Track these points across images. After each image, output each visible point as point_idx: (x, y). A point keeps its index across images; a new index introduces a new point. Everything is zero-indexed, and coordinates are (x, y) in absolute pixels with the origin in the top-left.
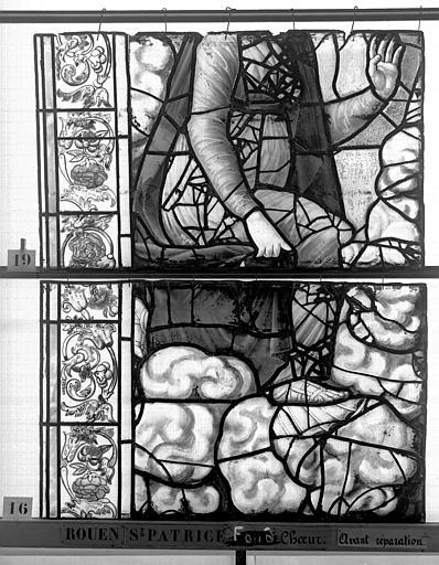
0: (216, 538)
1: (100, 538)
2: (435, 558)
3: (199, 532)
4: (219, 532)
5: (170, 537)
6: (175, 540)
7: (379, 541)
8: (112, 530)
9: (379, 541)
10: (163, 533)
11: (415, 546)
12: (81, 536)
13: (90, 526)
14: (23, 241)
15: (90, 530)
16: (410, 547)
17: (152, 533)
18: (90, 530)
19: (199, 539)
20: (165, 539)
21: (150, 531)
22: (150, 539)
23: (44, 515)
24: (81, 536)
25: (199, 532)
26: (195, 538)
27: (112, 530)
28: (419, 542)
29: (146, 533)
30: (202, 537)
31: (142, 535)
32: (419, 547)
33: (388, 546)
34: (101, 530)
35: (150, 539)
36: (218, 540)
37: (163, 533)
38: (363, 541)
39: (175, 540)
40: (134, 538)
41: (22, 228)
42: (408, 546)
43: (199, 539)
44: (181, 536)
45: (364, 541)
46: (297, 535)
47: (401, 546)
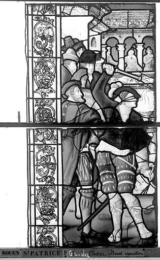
2: (159, 258)
9: (126, 254)
11: (140, 256)
14: (19, 112)
16: (138, 256)
17: (32, 253)
23: (30, 245)
29: (30, 253)
30: (52, 253)
32: (142, 256)
33: (129, 256)
38: (121, 254)
41: (15, 105)
42: (137, 256)
44: (43, 254)
45: (121, 254)
46: (95, 252)
47: (134, 256)
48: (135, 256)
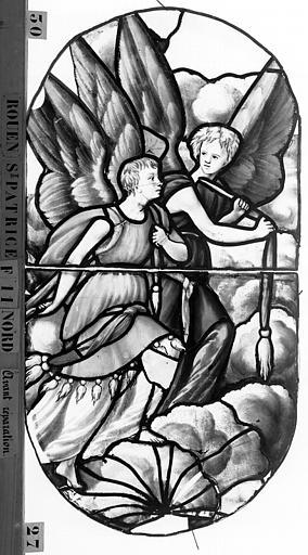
1: (8, 134)
3: (15, 232)
4: (15, 251)
5: (11, 203)
6: (7, 208)
7: (5, 410)
8: (17, 145)
10: (13, 197)
12: (10, 114)
15: (17, 123)
18: (17, 123)
19: (7, 232)
20: (7, 199)
22: (8, 183)
24: (10, 114)
25: (15, 232)
27: (17, 145)
31: (12, 176)
34: (16, 134)
35: (8, 183)
36: (7, 251)
37: (13, 197)
38: (6, 396)
39: (7, 208)
40: (9, 168)
43: (7, 232)
44: (11, 214)
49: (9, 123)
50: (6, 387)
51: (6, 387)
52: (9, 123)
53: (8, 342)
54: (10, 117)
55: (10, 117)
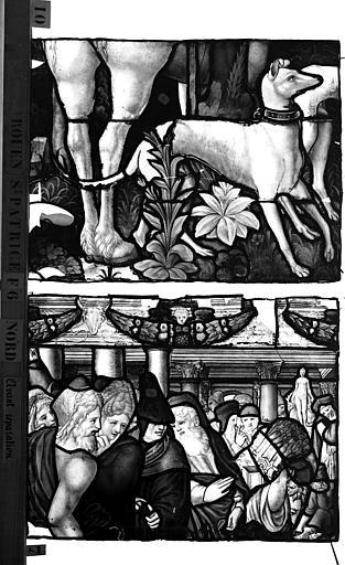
0: (12, 262)
1: (13, 152)
5: (14, 219)
6: (12, 223)
8: (20, 163)
13: (24, 141)
15: (20, 142)
18: (20, 142)
19: (11, 246)
20: (12, 214)
21: (19, 199)
22: (12, 199)
26: (15, 242)
27: (20, 163)
28: (9, 456)
30: (12, 249)
31: (16, 192)
35: (12, 199)
39: (12, 223)
43: (11, 246)
44: (15, 229)
48: (5, 440)
49: (13, 142)
50: (9, 391)
51: (9, 391)
52: (13, 142)
53: (11, 351)
54: (15, 136)
55: (15, 136)
